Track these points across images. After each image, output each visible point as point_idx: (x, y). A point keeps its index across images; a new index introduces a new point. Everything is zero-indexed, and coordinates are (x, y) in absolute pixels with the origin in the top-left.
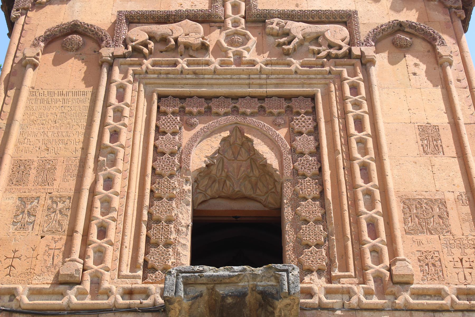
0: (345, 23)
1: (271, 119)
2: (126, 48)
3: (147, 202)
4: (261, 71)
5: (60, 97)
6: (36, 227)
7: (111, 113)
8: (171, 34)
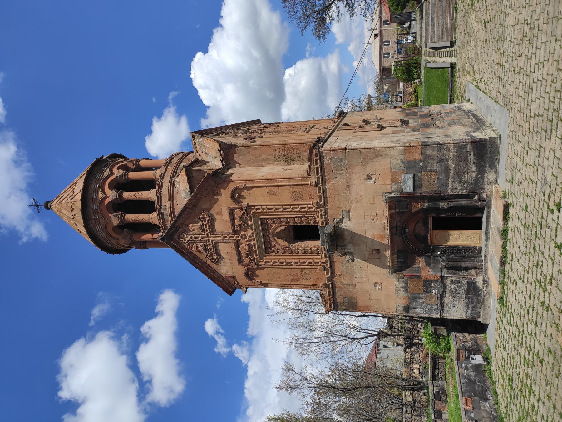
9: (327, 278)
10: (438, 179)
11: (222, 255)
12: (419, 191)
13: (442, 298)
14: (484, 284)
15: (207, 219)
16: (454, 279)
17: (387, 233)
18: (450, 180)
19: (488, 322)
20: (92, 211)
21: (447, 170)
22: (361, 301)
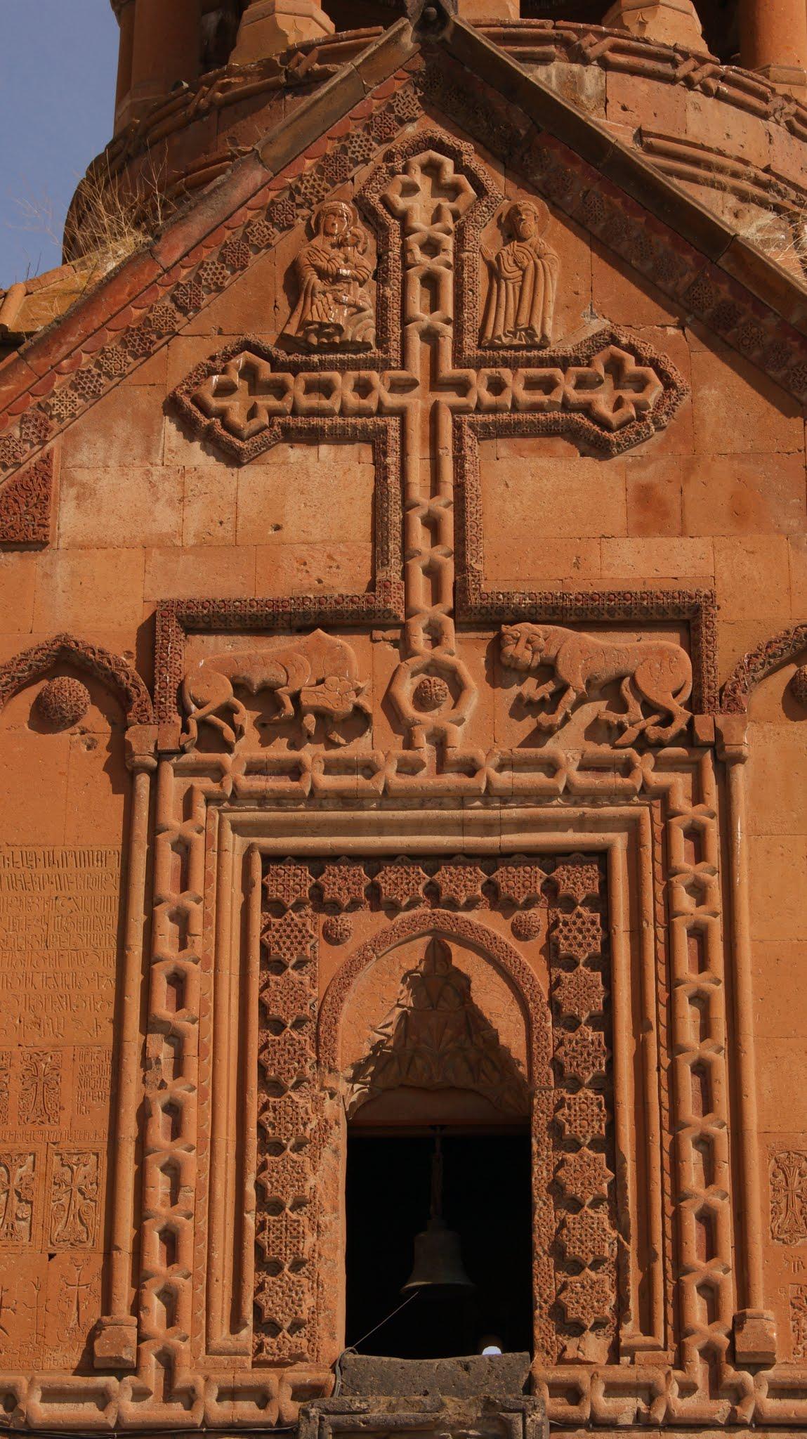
2: (186, 729)
5: (48, 870)
6: (38, 1231)
8: (283, 678)
15: (602, 401)
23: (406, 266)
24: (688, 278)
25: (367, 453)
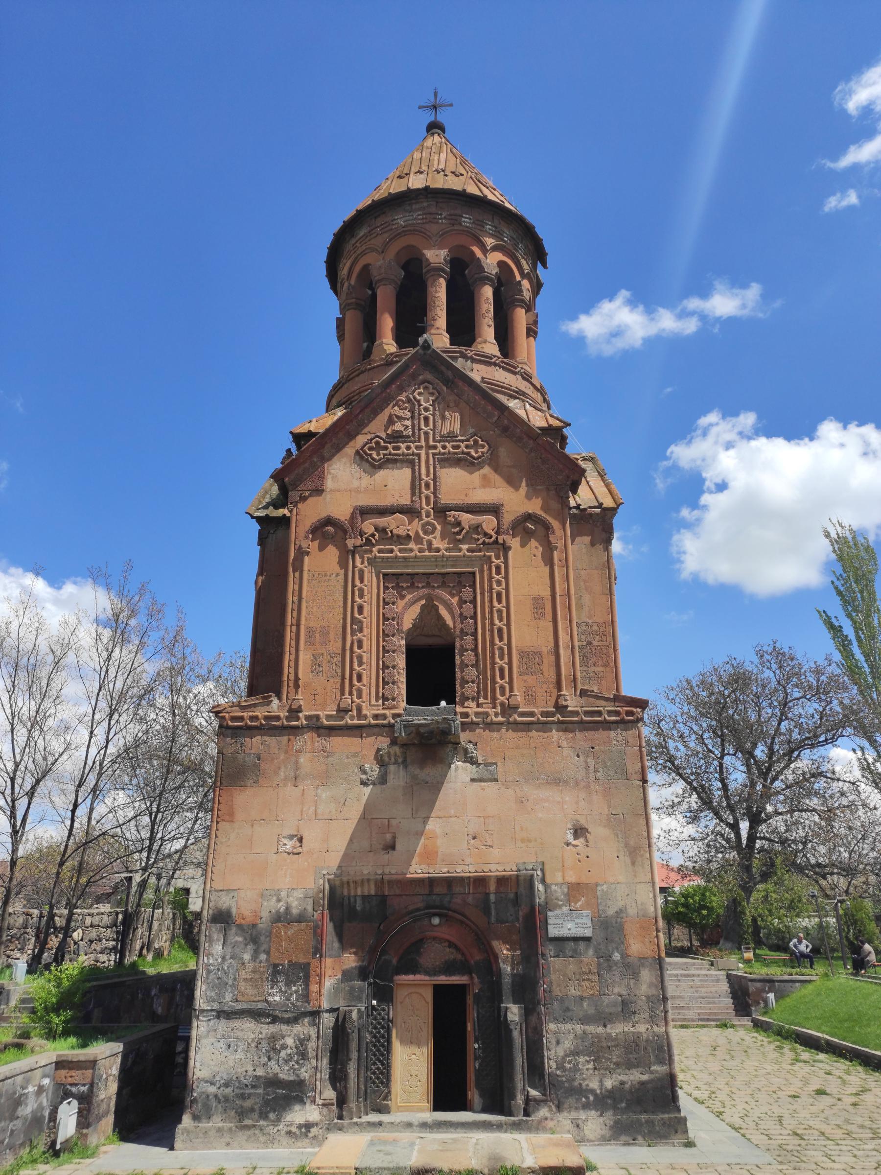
0: (496, 512)
1: (449, 589)
3: (381, 656)
4: (443, 556)
7: (357, 593)
9: (318, 717)
10: (582, 998)
11: (382, 473)
12: (550, 950)
13: (256, 1015)
14: (300, 1127)
15: (473, 452)
16: (311, 1045)
17: (440, 870)
18: (579, 1028)
19: (178, 1144)
20: (458, 212)
21: (604, 1019)
22: (246, 800)
23: (420, 415)
24: (496, 418)
25: (410, 465)
